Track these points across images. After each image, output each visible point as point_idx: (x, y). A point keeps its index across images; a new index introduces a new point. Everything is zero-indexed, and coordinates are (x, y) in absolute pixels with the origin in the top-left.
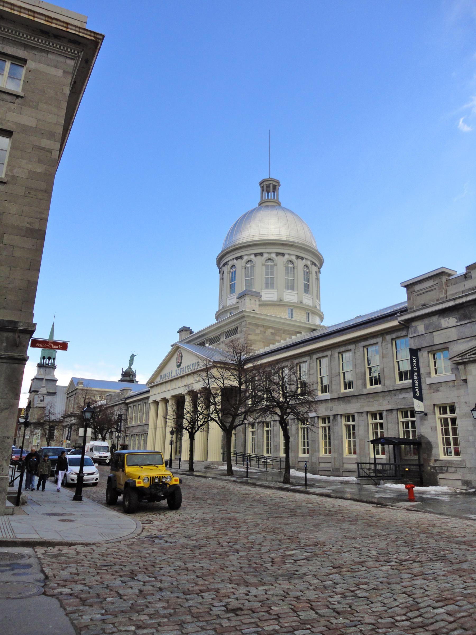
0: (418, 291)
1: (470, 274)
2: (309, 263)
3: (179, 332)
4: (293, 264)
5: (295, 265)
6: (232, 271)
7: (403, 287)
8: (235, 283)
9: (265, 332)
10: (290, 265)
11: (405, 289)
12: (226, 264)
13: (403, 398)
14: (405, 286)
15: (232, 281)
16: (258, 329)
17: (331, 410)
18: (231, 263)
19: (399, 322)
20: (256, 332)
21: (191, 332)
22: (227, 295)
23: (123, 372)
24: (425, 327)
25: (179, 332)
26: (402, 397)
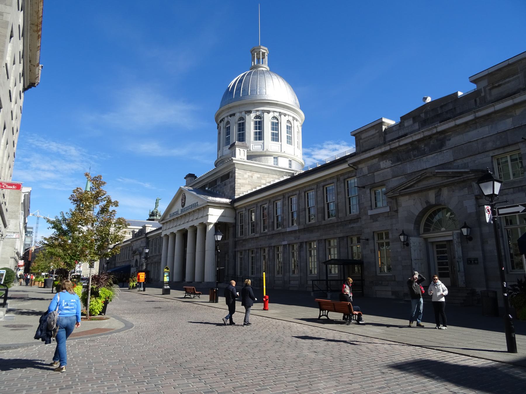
0: (364, 138)
1: (403, 123)
2: (291, 119)
3: (185, 178)
4: (278, 120)
5: (279, 121)
6: (227, 126)
7: (352, 135)
8: (229, 137)
9: (252, 177)
10: (275, 121)
11: (354, 137)
12: (222, 120)
13: (352, 227)
14: (354, 135)
15: (227, 135)
16: (246, 174)
17: (298, 239)
18: (226, 119)
19: (349, 165)
20: (245, 177)
21: (196, 177)
22: (223, 147)
23: (150, 212)
24: (368, 169)
25: (185, 178)
26: (351, 227)
